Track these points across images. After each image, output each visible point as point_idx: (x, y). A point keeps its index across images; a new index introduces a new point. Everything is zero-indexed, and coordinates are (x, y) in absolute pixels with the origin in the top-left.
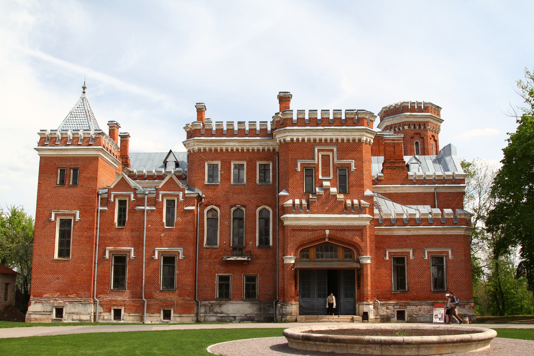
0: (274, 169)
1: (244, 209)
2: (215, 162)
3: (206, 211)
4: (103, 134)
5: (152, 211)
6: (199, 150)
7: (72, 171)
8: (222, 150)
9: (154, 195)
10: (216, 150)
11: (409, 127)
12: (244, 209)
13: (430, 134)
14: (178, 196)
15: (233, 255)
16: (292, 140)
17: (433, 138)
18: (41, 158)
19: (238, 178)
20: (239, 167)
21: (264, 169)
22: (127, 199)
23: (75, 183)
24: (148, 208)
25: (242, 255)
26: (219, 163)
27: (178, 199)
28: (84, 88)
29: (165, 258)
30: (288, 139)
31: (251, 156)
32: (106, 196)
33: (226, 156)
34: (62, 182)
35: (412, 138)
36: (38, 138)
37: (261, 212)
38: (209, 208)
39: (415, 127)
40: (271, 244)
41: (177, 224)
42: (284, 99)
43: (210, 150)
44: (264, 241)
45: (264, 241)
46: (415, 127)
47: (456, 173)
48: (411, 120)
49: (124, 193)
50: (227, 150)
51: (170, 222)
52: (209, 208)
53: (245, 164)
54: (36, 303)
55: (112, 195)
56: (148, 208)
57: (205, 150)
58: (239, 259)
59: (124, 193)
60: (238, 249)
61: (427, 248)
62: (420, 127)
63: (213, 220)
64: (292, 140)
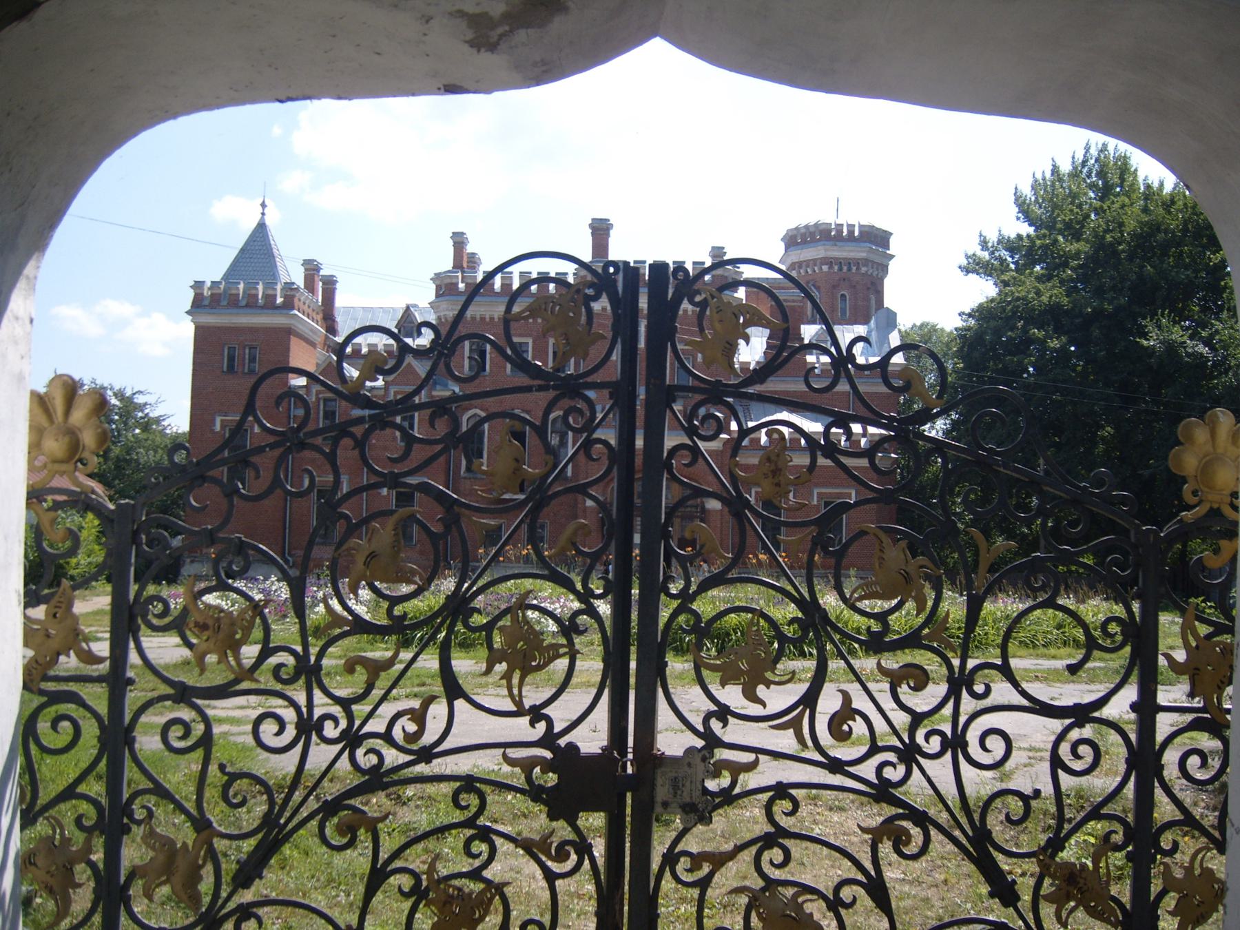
3: (465, 418)
4: (297, 289)
7: (247, 351)
9: (382, 392)
10: (483, 319)
11: (831, 267)
18: (197, 328)
28: (263, 205)
35: (834, 287)
36: (191, 295)
39: (840, 269)
42: (600, 230)
46: (840, 269)
53: (530, 341)
54: (192, 562)
55: (314, 391)
61: (817, 485)
62: (849, 269)
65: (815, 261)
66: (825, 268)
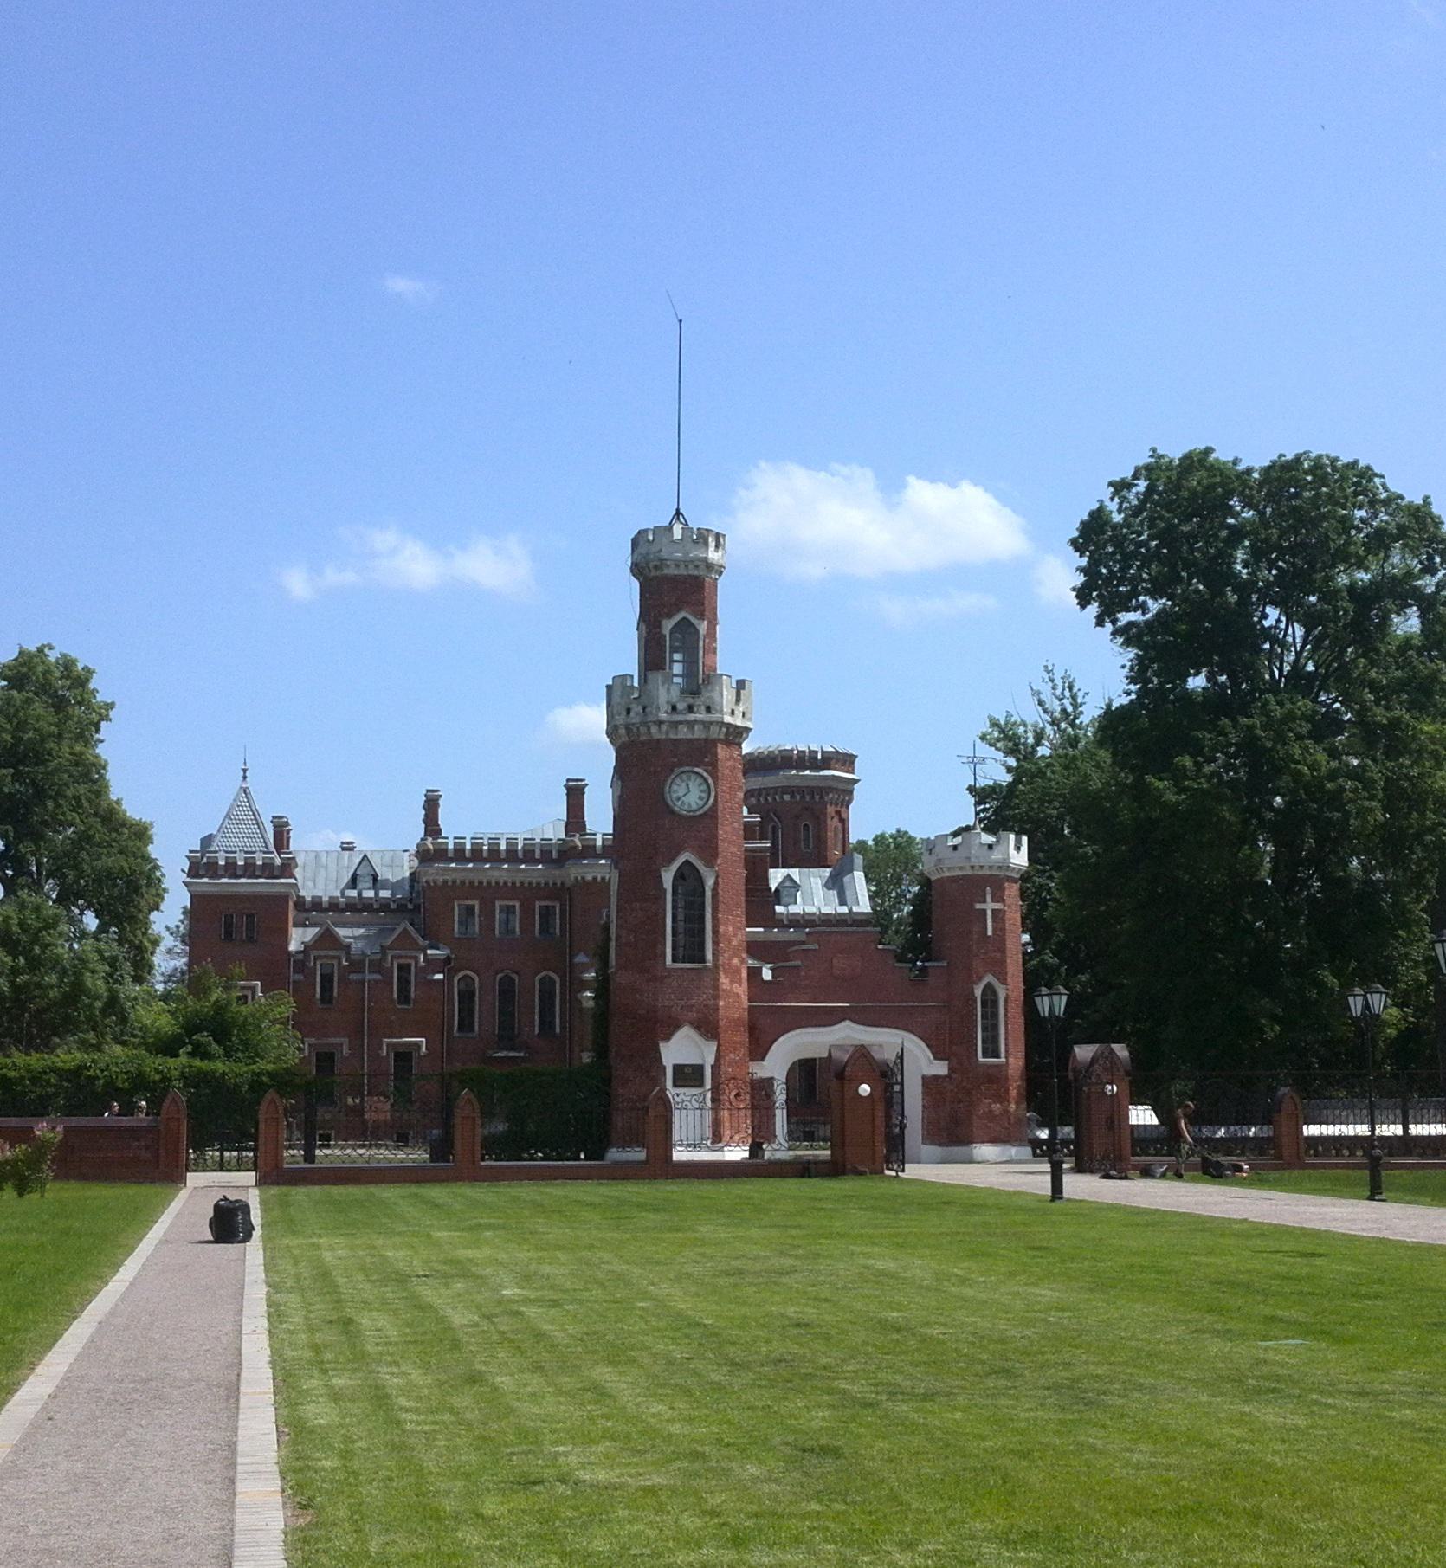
0: (562, 911)
1: (515, 976)
2: (470, 902)
5: (376, 981)
6: (445, 882)
8: (481, 883)
10: (472, 883)
12: (515, 976)
13: (831, 810)
14: (416, 959)
15: (502, 1049)
16: (595, 879)
17: (836, 819)
19: (508, 930)
20: (509, 910)
21: (547, 914)
22: (335, 962)
23: (250, 939)
24: (368, 976)
25: (513, 1049)
26: (476, 903)
27: (417, 963)
29: (397, 1055)
30: (589, 877)
31: (526, 893)
32: (301, 956)
33: (488, 892)
34: (228, 934)
35: (797, 817)
37: (542, 981)
38: (461, 974)
39: (803, 797)
40: (558, 1030)
41: (415, 1001)
43: (463, 883)
44: (547, 1024)
45: (547, 1024)
46: (803, 797)
47: (855, 909)
48: (797, 782)
49: (331, 953)
50: (489, 883)
51: (404, 996)
52: (461, 974)
56: (368, 976)
57: (454, 882)
58: (512, 1054)
59: (331, 953)
60: (507, 1037)
62: (813, 797)
63: (467, 997)
64: (595, 879)
65: (776, 789)
66: (787, 797)
